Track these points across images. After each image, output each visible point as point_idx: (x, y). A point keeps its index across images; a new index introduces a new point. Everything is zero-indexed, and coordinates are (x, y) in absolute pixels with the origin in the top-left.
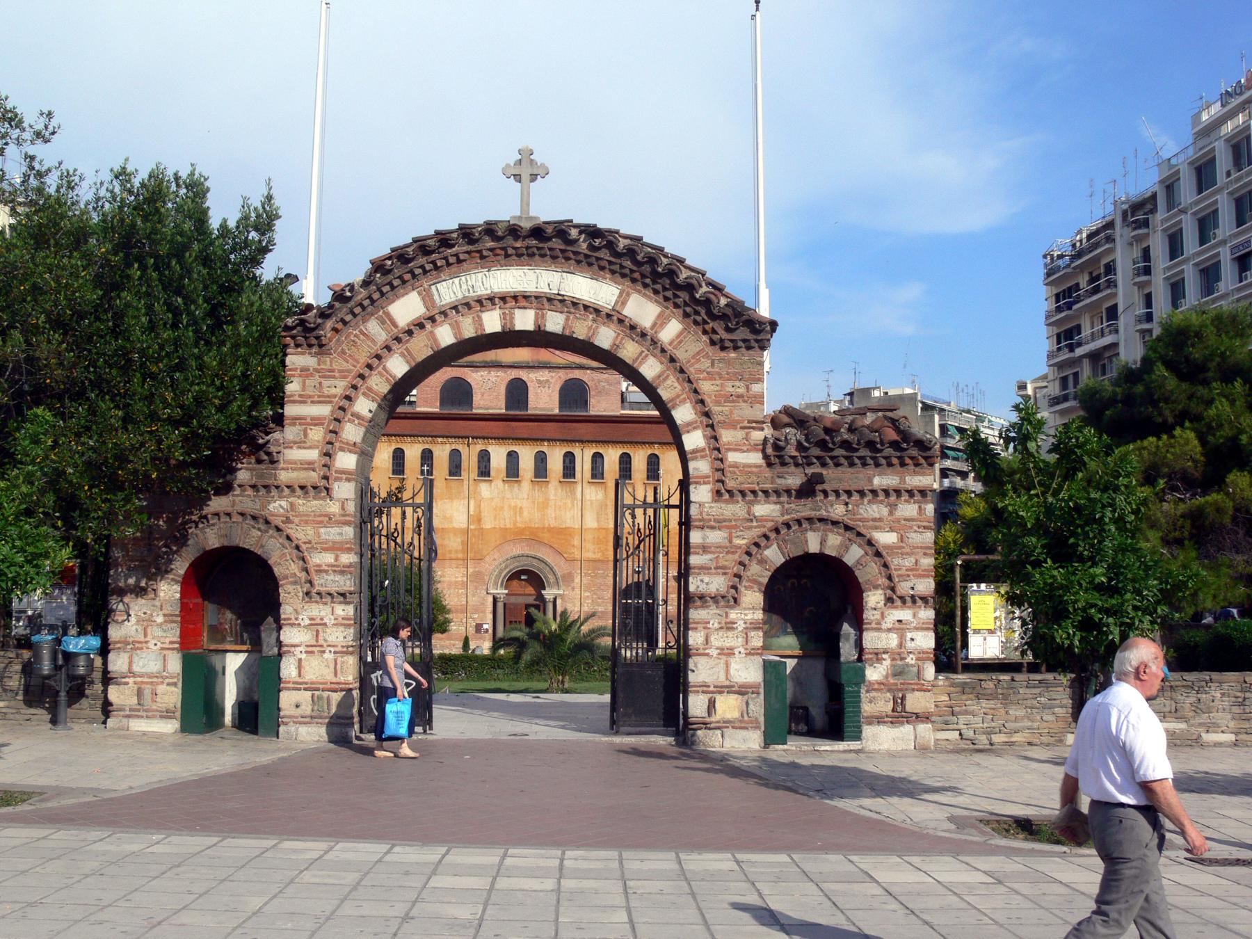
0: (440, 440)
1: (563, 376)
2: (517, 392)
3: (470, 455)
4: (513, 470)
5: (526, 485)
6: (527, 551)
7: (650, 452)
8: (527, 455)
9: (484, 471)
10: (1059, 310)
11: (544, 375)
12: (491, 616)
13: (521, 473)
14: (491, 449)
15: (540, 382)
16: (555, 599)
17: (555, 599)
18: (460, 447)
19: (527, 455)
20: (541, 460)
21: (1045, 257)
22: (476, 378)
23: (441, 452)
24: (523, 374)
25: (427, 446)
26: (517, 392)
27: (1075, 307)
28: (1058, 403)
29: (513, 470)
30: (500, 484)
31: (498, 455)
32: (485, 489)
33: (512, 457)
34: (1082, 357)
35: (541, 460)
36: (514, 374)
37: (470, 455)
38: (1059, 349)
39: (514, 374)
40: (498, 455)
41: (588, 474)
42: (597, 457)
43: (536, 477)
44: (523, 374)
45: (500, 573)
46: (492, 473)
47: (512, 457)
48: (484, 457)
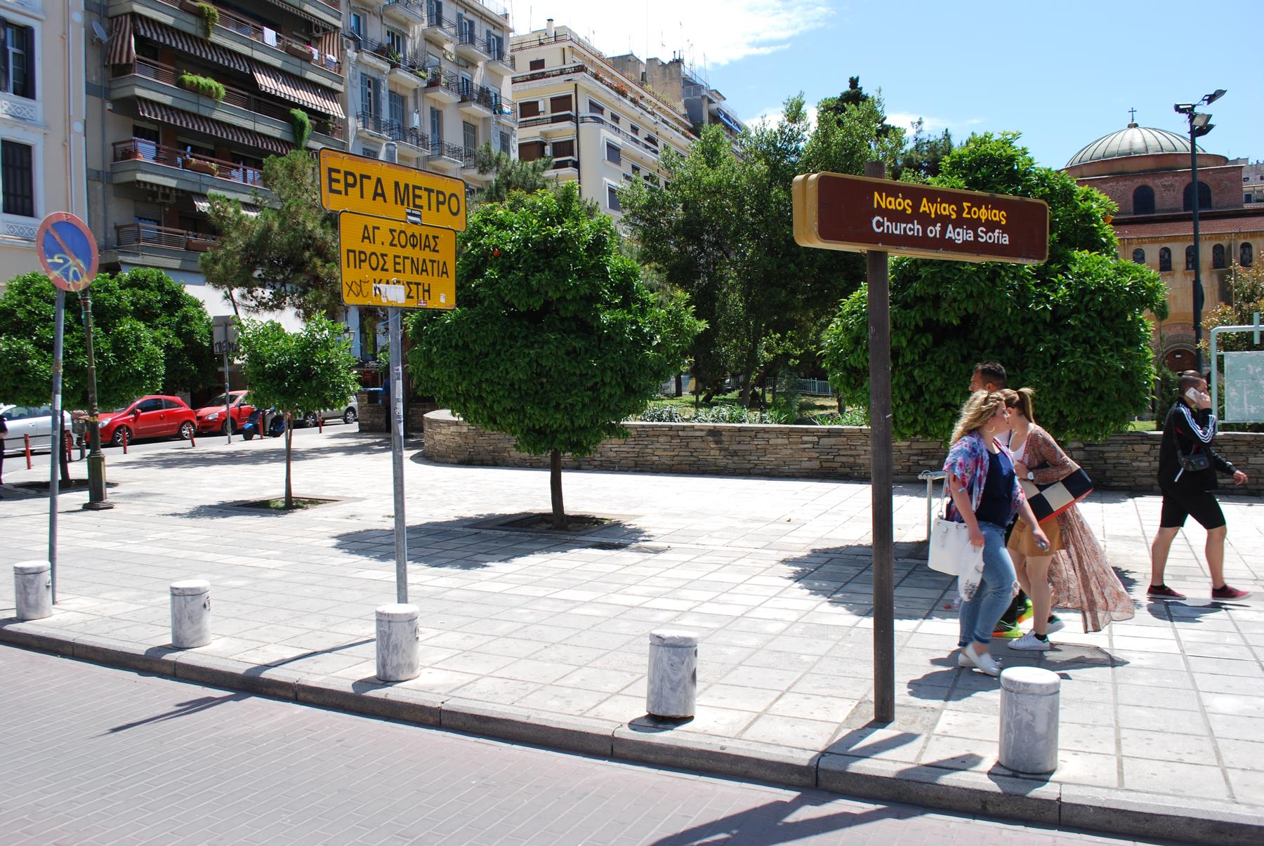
6: (1181, 332)
11: (1167, 180)
14: (1144, 247)
15: (1164, 186)
24: (1149, 182)
39: (1139, 182)
44: (1149, 182)
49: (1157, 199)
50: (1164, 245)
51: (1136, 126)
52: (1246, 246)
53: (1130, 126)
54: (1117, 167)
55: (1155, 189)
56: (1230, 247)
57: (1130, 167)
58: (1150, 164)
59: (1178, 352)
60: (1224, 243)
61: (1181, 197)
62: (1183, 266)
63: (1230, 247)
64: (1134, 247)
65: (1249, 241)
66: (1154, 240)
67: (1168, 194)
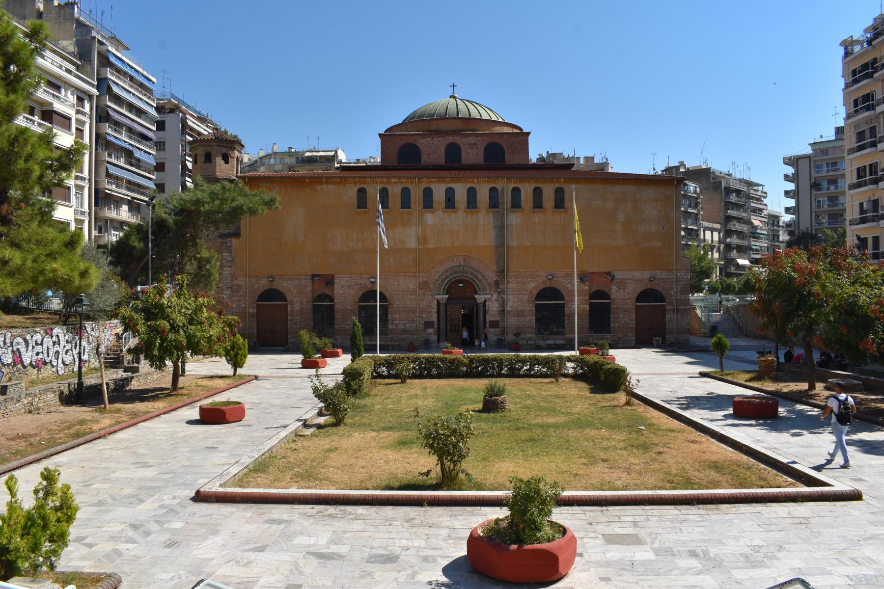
0: (394, 180)
1: (487, 140)
2: (453, 152)
3: (416, 194)
4: (450, 202)
5: (460, 213)
6: (462, 263)
7: (557, 185)
8: (461, 191)
9: (428, 202)
10: (856, 81)
11: (472, 140)
12: (436, 315)
13: (457, 205)
14: (432, 186)
15: (469, 144)
16: (485, 302)
17: (485, 302)
18: (409, 186)
19: (461, 191)
20: (472, 194)
21: (841, 45)
22: (423, 144)
23: (395, 190)
24: (458, 140)
25: (383, 186)
26: (453, 152)
27: (875, 75)
28: (853, 153)
29: (450, 202)
30: (441, 213)
31: (439, 191)
32: (430, 218)
33: (450, 193)
34: (880, 113)
35: (472, 193)
36: (449, 139)
37: (416, 194)
38: (856, 111)
39: (449, 139)
40: (439, 191)
41: (510, 205)
42: (516, 191)
43: (468, 207)
45: (443, 281)
46: (435, 205)
47: (450, 193)
48: (428, 193)
49: (464, 155)
50: (450, 185)
51: (455, 97)
52: (516, 190)
53: (451, 97)
54: (434, 127)
55: (462, 146)
56: (503, 189)
57: (444, 126)
58: (458, 125)
59: (461, 281)
60: (499, 186)
61: (482, 154)
62: (465, 205)
63: (503, 189)
64: (424, 185)
65: (518, 185)
66: (441, 180)
67: (472, 154)
